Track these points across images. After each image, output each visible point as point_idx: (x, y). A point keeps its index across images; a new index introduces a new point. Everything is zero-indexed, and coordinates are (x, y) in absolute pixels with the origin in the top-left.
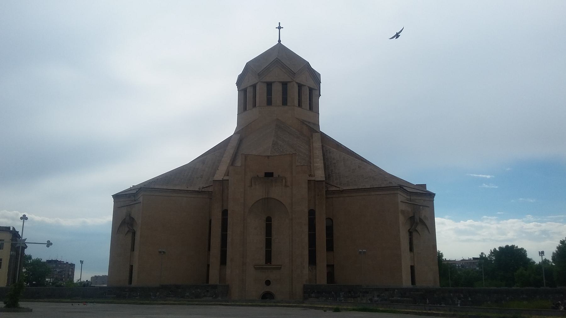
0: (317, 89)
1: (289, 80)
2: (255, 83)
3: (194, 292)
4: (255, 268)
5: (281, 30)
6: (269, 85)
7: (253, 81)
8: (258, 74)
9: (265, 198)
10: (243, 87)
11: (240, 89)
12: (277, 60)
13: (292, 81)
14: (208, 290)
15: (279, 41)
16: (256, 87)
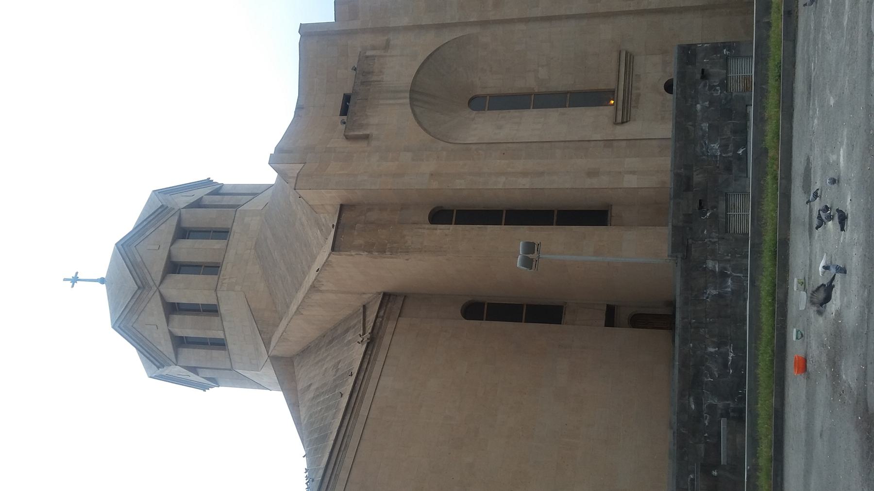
0: (219, 186)
1: (174, 222)
2: (160, 304)
3: (705, 126)
4: (623, 123)
5: (80, 276)
6: (174, 267)
7: (155, 311)
8: (139, 288)
9: (411, 99)
10: (167, 347)
11: (173, 357)
12: (122, 245)
13: (179, 212)
14: (698, 76)
15: (102, 281)
16: (173, 304)
